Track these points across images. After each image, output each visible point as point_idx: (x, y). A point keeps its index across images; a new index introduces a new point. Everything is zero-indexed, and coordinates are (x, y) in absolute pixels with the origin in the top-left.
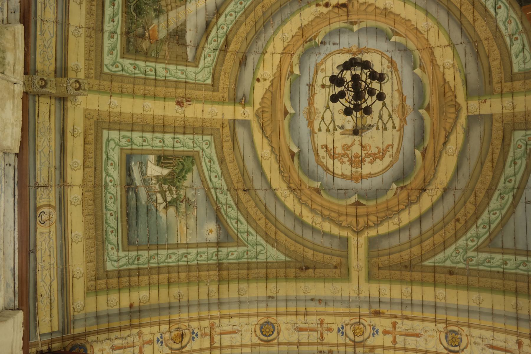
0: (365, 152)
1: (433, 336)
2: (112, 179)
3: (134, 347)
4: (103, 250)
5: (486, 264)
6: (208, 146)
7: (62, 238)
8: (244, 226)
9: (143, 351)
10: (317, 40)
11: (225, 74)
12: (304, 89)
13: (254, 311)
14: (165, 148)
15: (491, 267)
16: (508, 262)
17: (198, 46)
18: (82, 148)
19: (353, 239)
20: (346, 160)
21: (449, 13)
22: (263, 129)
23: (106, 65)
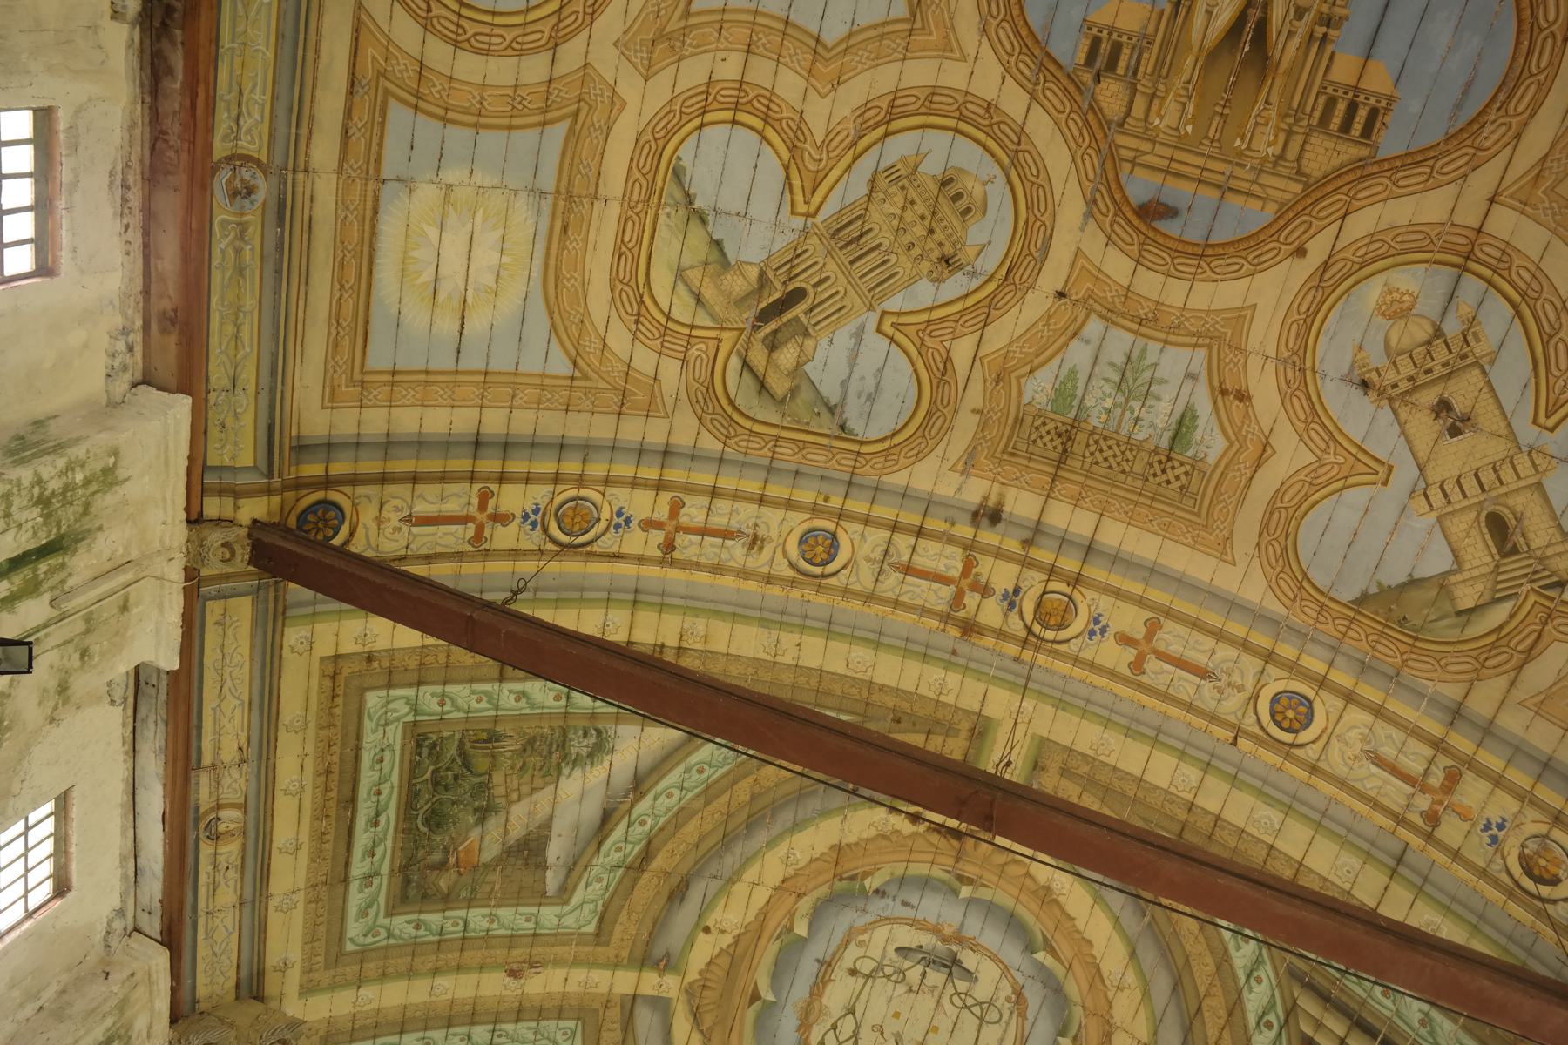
10: (867, 882)
11: (630, 914)
12: (808, 968)
17: (575, 864)
21: (1177, 987)
22: (696, 1015)
23: (351, 940)
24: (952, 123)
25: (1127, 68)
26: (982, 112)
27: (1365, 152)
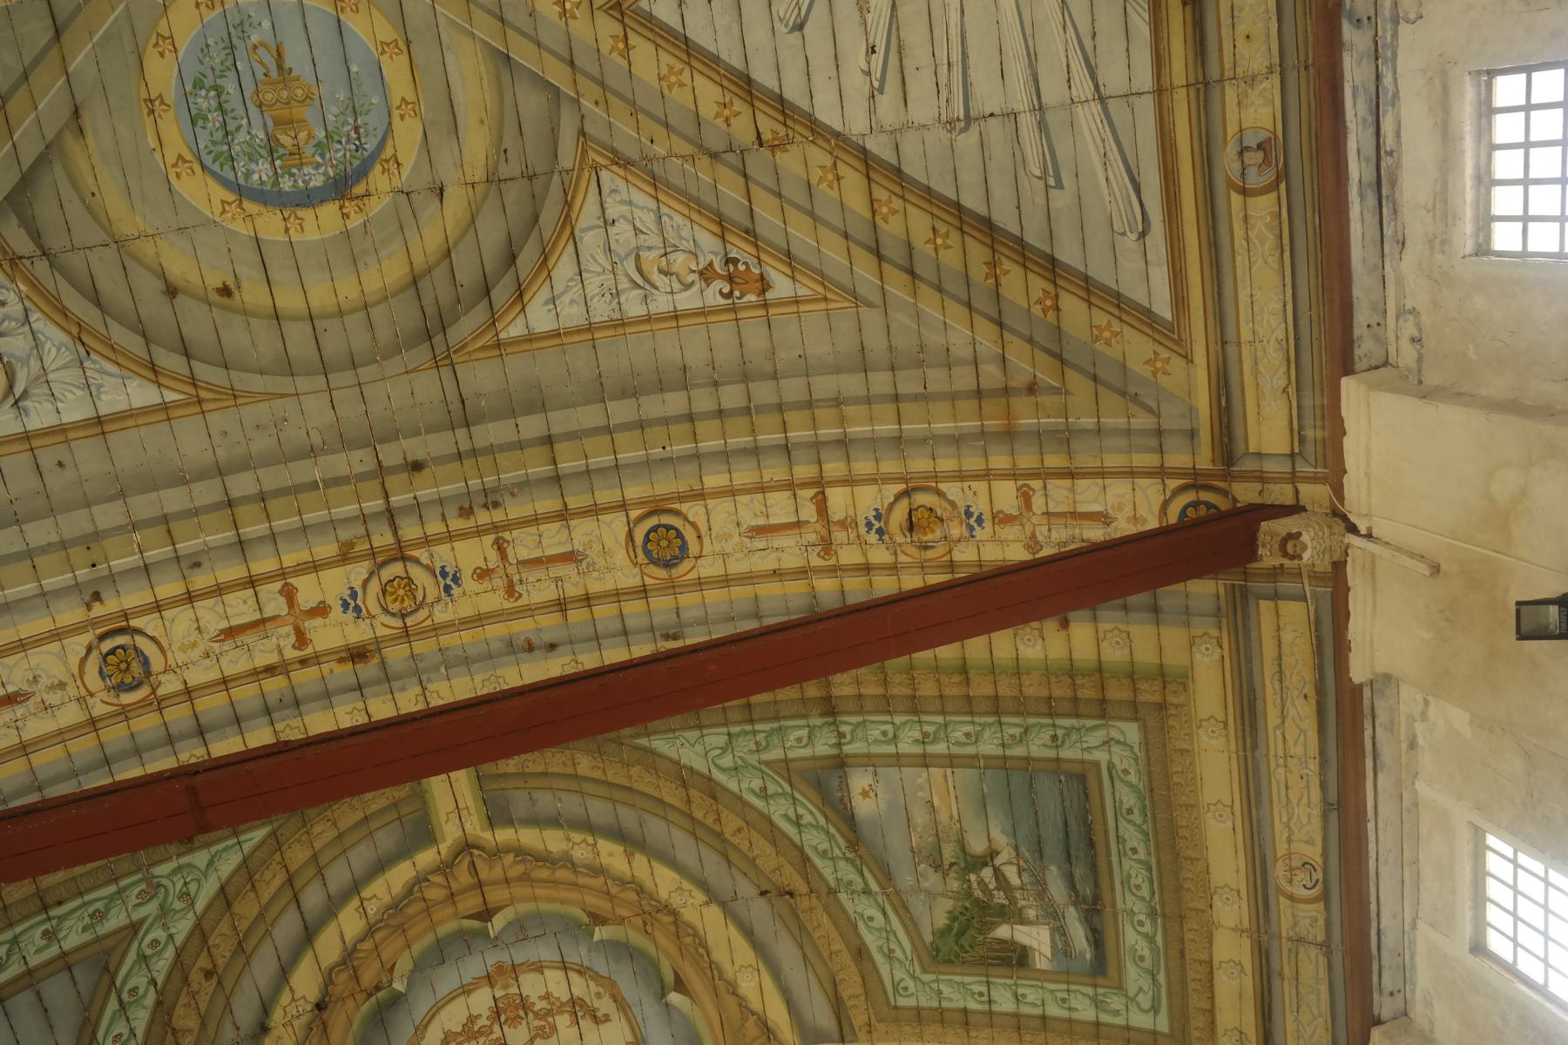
0: (494, 1036)
1: (183, 649)
2: (1139, 928)
3: (1047, 513)
4: (1150, 774)
5: (99, 905)
6: (902, 985)
7: (1259, 822)
8: (778, 810)
9: (1021, 500)
13: (714, 596)
14: (1009, 982)
15: (85, 904)
16: (44, 942)
18: (1217, 1000)
19: (475, 826)
20: (540, 1005)
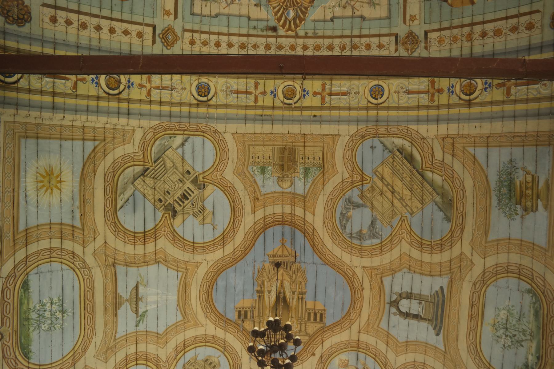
24: (204, 344)
25: (250, 316)
26: (212, 339)
27: (322, 325)
